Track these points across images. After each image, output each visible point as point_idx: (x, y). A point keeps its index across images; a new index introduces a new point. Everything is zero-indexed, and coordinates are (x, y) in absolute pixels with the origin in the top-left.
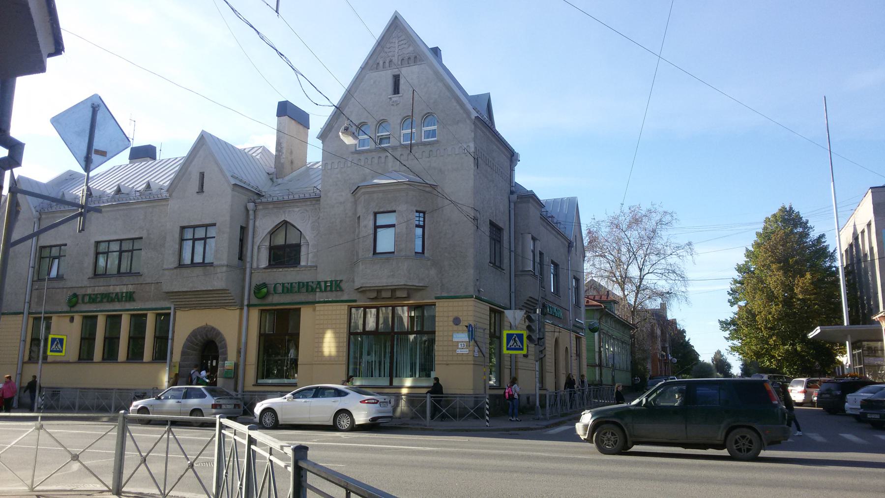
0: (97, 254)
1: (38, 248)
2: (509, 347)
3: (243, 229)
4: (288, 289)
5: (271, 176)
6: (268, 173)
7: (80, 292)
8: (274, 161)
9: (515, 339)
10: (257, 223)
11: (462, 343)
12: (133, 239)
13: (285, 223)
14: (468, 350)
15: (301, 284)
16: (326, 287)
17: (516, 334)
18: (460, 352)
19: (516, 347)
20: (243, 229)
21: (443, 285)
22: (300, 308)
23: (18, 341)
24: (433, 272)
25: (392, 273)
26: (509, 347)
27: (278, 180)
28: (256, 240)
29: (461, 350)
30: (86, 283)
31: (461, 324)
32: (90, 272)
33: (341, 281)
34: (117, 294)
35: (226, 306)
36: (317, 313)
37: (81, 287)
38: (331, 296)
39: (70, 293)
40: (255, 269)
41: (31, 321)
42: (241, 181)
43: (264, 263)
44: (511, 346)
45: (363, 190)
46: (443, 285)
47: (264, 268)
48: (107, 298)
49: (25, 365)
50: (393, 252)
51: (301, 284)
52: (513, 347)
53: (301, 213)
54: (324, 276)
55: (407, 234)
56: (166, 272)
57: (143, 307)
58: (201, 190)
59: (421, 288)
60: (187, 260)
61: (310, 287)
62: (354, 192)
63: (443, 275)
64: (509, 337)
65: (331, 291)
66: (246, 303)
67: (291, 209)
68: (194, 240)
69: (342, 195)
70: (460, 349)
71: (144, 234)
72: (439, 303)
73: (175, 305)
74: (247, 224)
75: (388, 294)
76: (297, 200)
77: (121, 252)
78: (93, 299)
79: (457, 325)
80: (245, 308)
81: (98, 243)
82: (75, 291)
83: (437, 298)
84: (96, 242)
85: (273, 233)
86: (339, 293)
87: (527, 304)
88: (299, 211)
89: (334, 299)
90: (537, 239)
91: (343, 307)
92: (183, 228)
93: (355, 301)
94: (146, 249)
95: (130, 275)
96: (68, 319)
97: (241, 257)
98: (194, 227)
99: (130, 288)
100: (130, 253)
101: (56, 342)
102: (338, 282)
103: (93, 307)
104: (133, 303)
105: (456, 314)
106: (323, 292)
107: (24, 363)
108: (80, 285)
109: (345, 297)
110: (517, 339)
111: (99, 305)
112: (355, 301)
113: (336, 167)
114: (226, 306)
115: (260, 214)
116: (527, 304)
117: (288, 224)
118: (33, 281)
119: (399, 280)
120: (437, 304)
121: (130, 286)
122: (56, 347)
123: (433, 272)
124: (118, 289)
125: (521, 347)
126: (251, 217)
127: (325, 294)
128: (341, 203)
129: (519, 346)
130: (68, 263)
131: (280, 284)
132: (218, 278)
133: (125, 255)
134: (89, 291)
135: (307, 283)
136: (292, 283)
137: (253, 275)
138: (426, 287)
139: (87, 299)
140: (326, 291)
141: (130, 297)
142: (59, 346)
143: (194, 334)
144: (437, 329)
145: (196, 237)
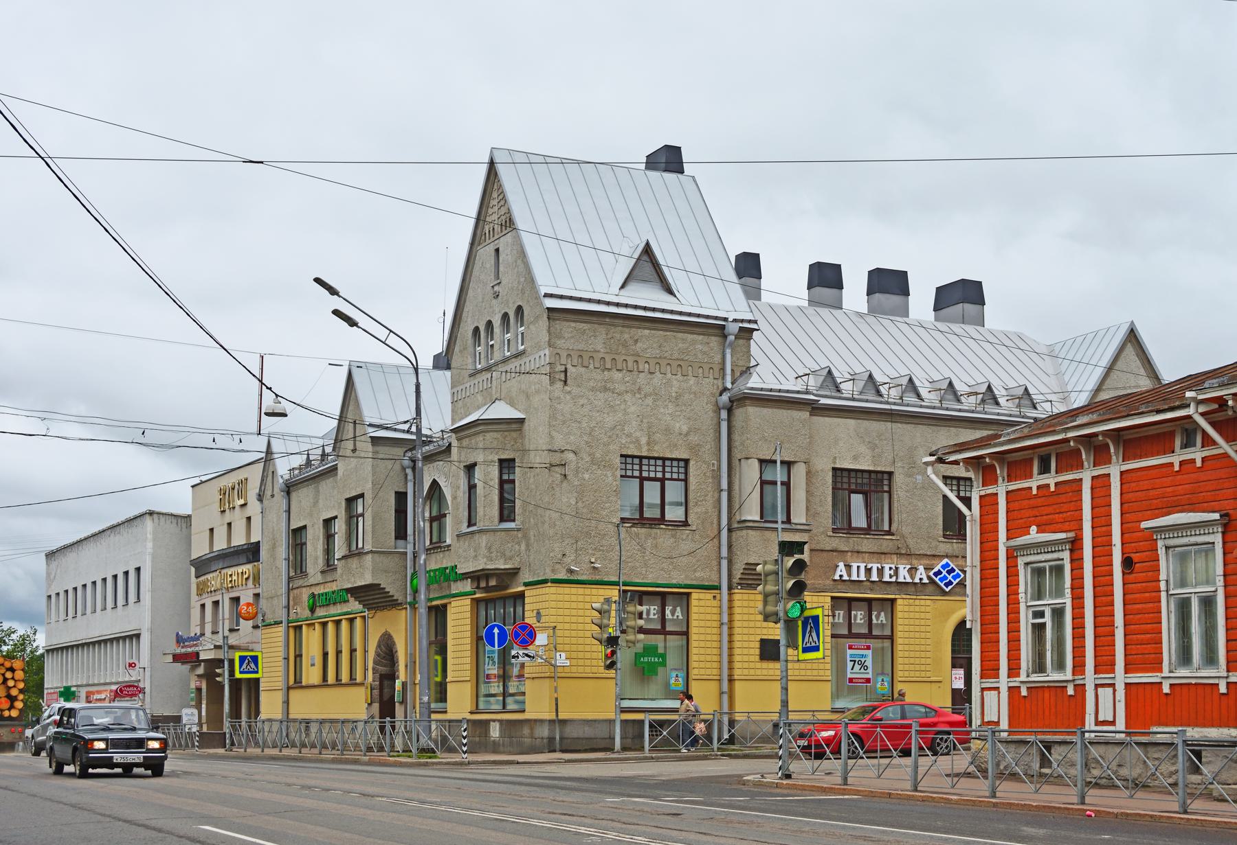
41: (292, 632)
49: (292, 693)
55: (485, 497)
72: (530, 593)
84: (324, 520)
87: (746, 574)
90: (795, 462)
101: (247, 661)
107: (289, 688)
116: (746, 574)
118: (289, 578)
142: (253, 665)
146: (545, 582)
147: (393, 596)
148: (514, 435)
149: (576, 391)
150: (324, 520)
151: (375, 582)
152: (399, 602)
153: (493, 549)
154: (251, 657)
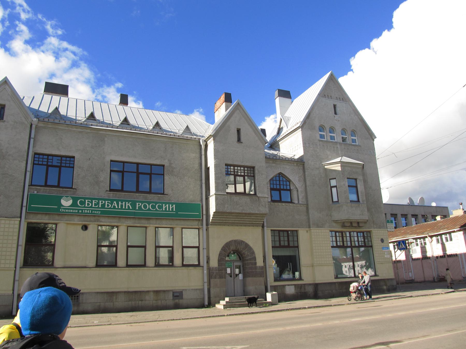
1: (33, 154)
18: (386, 257)
29: (387, 256)
58: (239, 140)
88: (289, 168)
94: (169, 175)
105: (382, 237)
120: (373, 231)
128: (317, 168)
130: (79, 175)
132: (262, 205)
143: (227, 245)
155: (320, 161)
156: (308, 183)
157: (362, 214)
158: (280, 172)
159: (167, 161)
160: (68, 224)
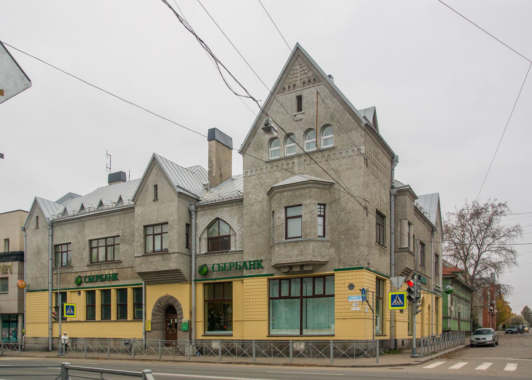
0: (91, 248)
2: (393, 304)
3: (188, 226)
4: (223, 268)
5: (206, 186)
6: (204, 185)
7: (83, 275)
8: (207, 176)
9: (397, 298)
10: (197, 221)
11: (356, 303)
12: (114, 237)
13: (218, 219)
14: (360, 308)
15: (232, 264)
16: (251, 265)
17: (399, 295)
19: (399, 304)
20: (188, 226)
21: (340, 260)
22: (231, 282)
23: (48, 308)
24: (332, 251)
25: (300, 253)
26: (393, 304)
27: (211, 189)
28: (197, 233)
29: (356, 308)
30: (86, 269)
31: (354, 289)
32: (87, 261)
33: (262, 261)
34: (106, 275)
35: (179, 281)
36: (245, 284)
37: (83, 271)
38: (255, 272)
39: (77, 275)
40: (198, 255)
41: (54, 295)
42: (184, 189)
43: (204, 250)
44: (394, 304)
45: (276, 190)
46: (340, 260)
47: (205, 254)
48: (101, 278)
50: (301, 237)
51: (232, 264)
52: (396, 304)
53: (229, 211)
54: (248, 257)
56: (137, 259)
57: (124, 284)
59: (323, 263)
60: (150, 248)
61: (238, 266)
62: (269, 193)
63: (340, 253)
64: (393, 297)
65: (254, 268)
66: (193, 278)
67: (221, 209)
68: (154, 235)
69: (259, 196)
70: (354, 307)
71: (120, 233)
72: (337, 274)
73: (145, 282)
74: (191, 221)
75: (298, 269)
76: (226, 202)
77: (106, 246)
78: (92, 279)
79: (351, 289)
80: (193, 282)
81: (91, 241)
82: (79, 274)
83: (335, 270)
85: (209, 227)
86: (260, 270)
88: (228, 210)
89: (257, 274)
91: (263, 280)
92: (145, 227)
93: (273, 275)
95: (114, 262)
96: (77, 293)
97: (188, 246)
98: (153, 225)
99: (115, 271)
100: (113, 247)
101: (69, 309)
102: (259, 261)
103: (91, 285)
104: (117, 281)
105: (351, 282)
106: (248, 269)
108: (82, 270)
109: (265, 272)
110: (399, 298)
111: (96, 283)
112: (273, 275)
113: (254, 174)
114: (179, 281)
115: (199, 214)
117: (220, 220)
118: (52, 269)
119: (306, 257)
120: (336, 275)
121: (115, 270)
122: (70, 312)
123: (332, 251)
124: (107, 272)
125: (402, 304)
126: (193, 216)
127: (249, 271)
128: (259, 202)
129: (401, 303)
131: (217, 264)
132: (172, 261)
133: (109, 248)
134: (88, 274)
135: (236, 263)
136: (225, 264)
137: (197, 258)
138: (327, 262)
139: (87, 280)
140: (250, 269)
141: (115, 277)
142: (72, 311)
144: (336, 293)
145: (155, 233)
146: (362, 268)
147: (185, 277)
148: (326, 191)
149: (368, 170)
150: (89, 240)
151: (179, 269)
152: (187, 280)
153: (315, 251)
154: (71, 306)
155: (265, 189)
156: (245, 223)
157: (301, 254)
158: (216, 217)
159: (121, 231)
160: (71, 292)
